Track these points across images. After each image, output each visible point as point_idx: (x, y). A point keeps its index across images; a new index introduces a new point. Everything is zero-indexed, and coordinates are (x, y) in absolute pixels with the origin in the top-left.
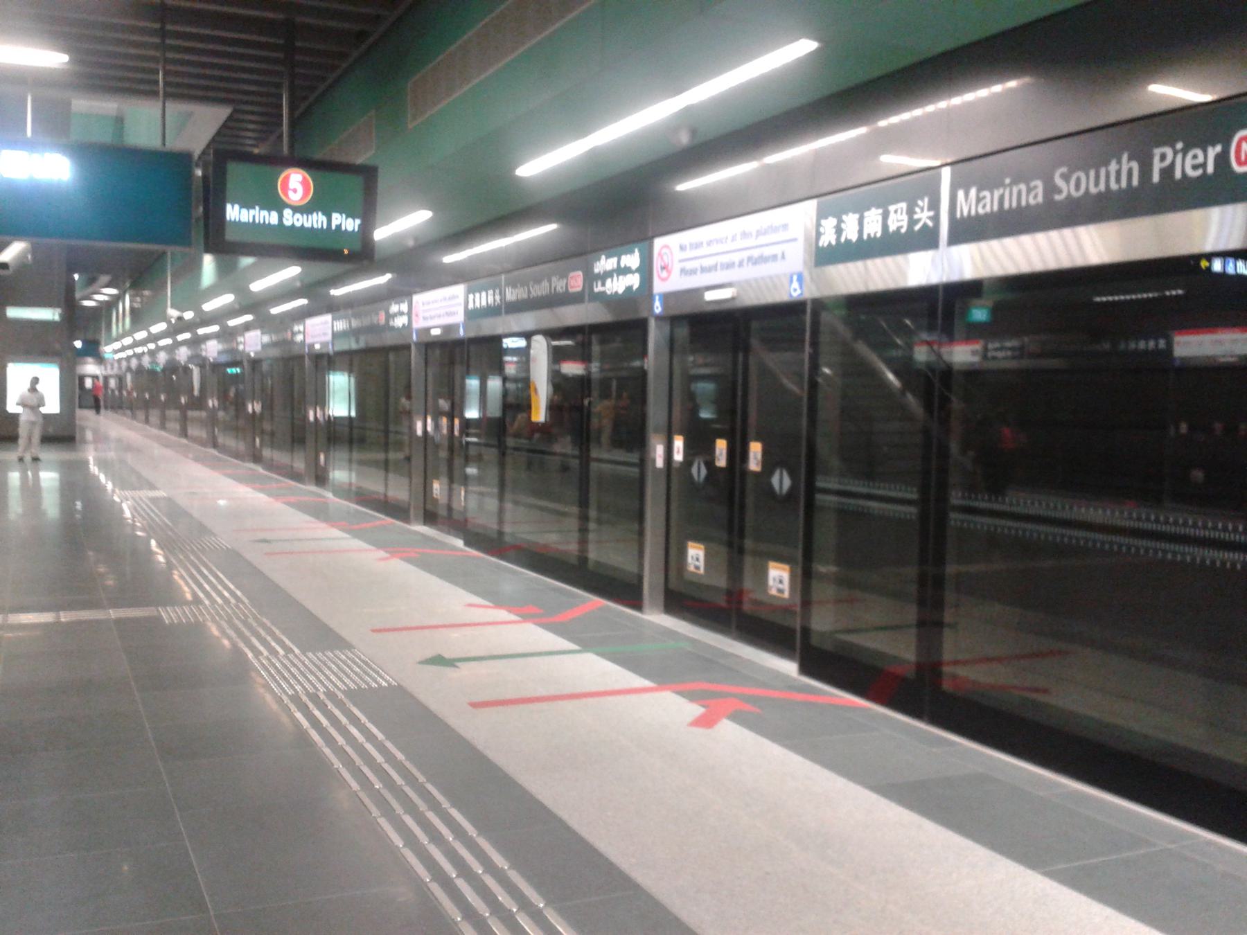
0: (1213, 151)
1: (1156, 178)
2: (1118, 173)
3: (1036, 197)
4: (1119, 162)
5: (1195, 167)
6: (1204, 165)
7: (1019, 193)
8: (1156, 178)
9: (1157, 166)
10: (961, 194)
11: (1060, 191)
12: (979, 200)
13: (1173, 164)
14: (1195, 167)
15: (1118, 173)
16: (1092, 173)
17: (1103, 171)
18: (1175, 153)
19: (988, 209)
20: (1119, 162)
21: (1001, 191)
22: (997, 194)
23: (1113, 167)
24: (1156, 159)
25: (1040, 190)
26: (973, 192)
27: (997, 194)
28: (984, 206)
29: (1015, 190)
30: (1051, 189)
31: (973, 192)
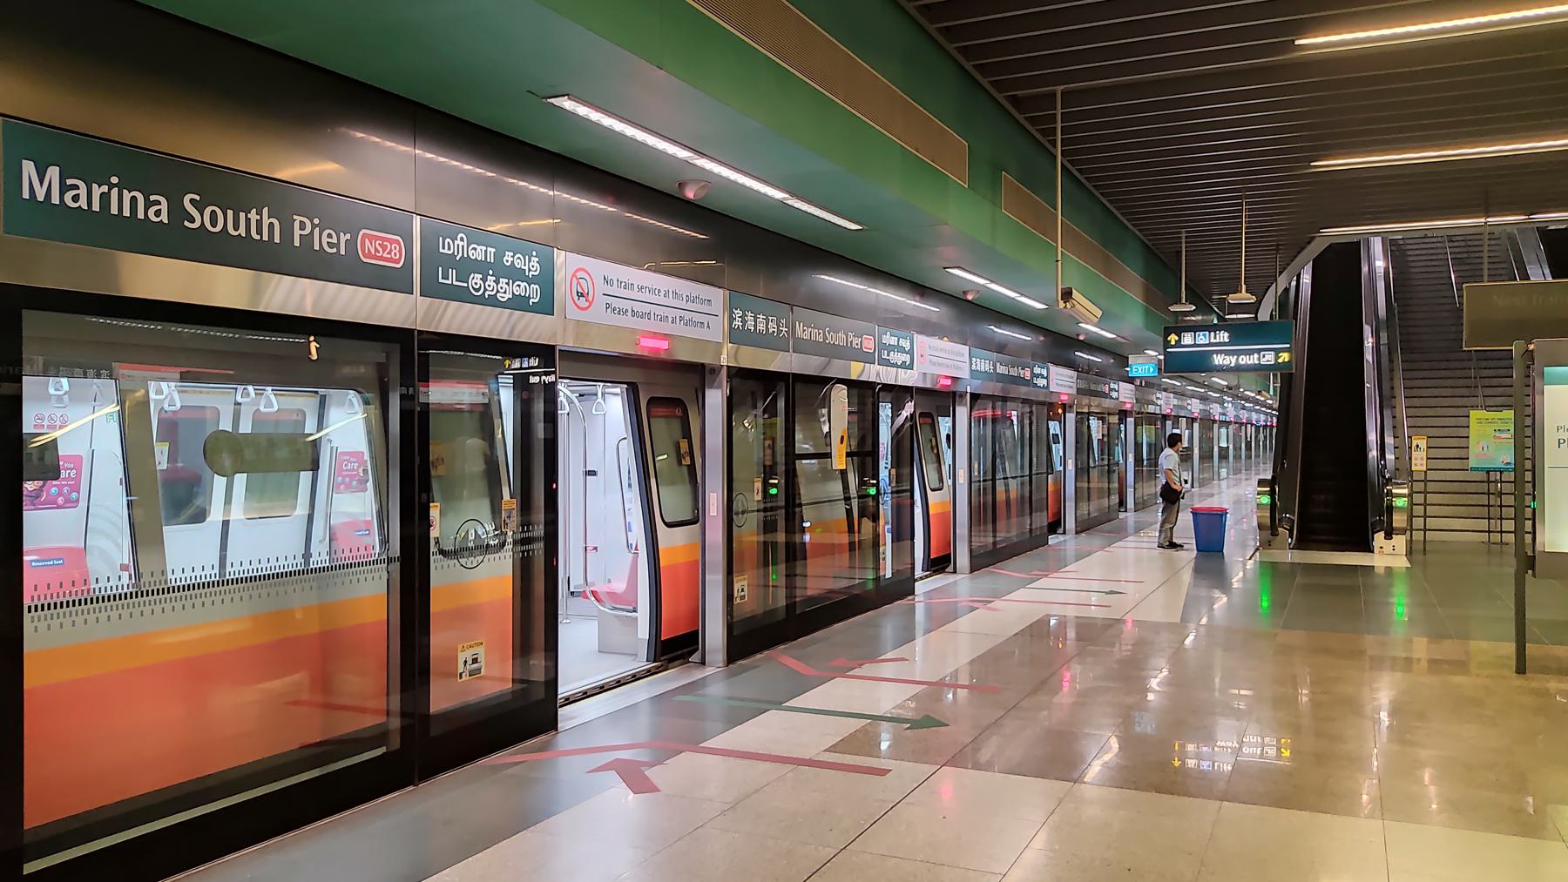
0: (343, 238)
1: (297, 243)
2: (259, 223)
3: (158, 213)
4: (260, 213)
5: (330, 245)
6: (337, 245)
7: (134, 199)
8: (297, 243)
9: (297, 232)
10: (28, 168)
11: (193, 221)
12: (64, 189)
13: (312, 232)
14: (330, 245)
15: (259, 223)
16: (230, 213)
17: (242, 215)
18: (314, 226)
19: (83, 203)
20: (260, 213)
21: (105, 188)
22: (97, 191)
23: (253, 216)
24: (297, 225)
25: (164, 207)
26: (53, 173)
27: (97, 191)
28: (76, 198)
29: (127, 196)
30: (177, 212)
31: (53, 173)
